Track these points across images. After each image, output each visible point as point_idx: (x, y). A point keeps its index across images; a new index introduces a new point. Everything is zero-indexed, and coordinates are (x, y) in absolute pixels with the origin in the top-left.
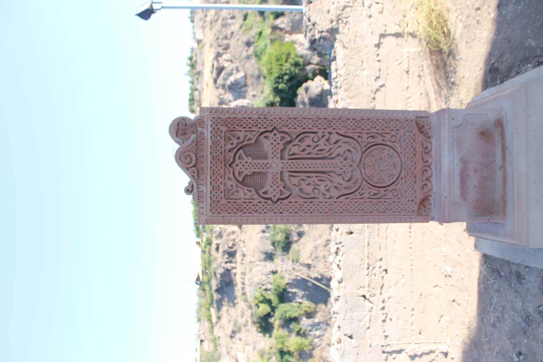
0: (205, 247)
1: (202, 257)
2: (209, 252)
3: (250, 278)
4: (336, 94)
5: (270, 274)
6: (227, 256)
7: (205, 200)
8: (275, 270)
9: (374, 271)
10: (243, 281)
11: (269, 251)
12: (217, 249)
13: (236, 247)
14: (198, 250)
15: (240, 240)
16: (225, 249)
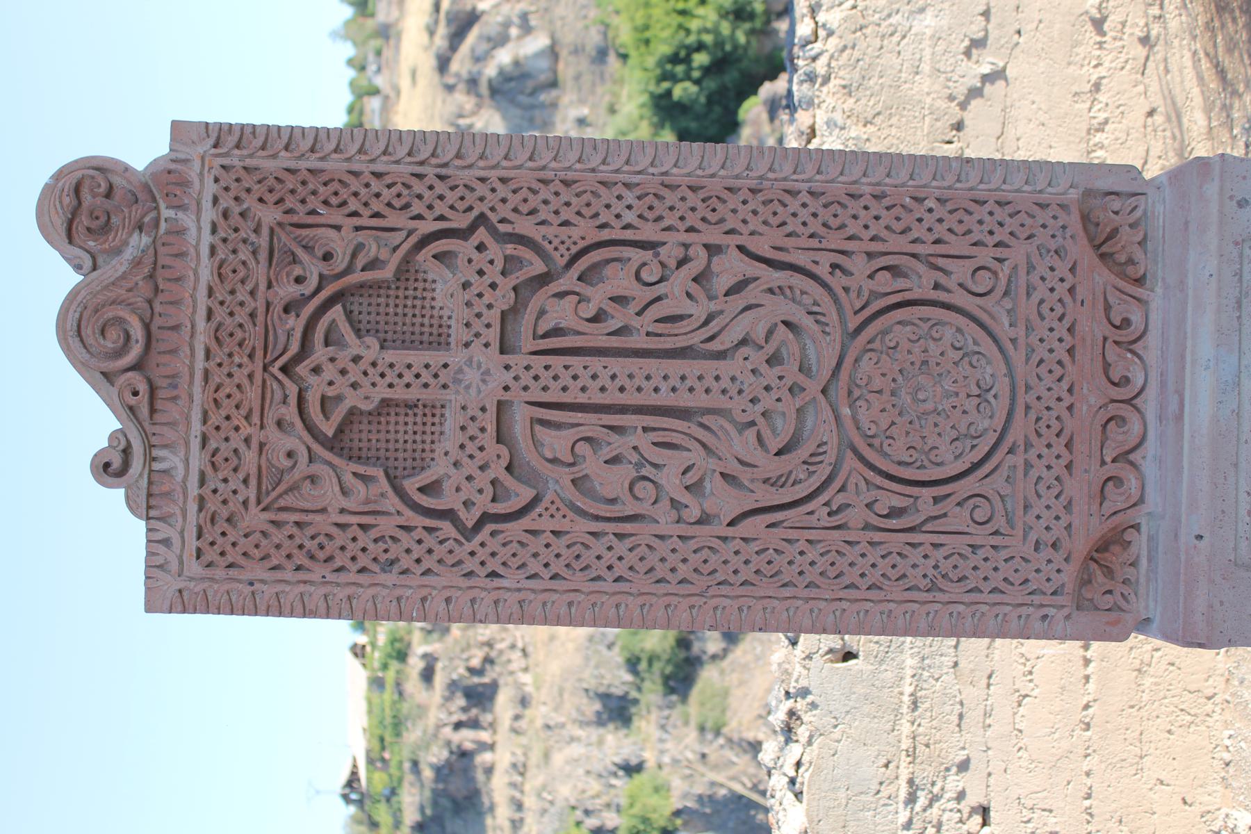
0: (385, 666)
1: (370, 702)
2: (398, 684)
3: (544, 787)
4: (810, 104)
5: (615, 775)
6: (461, 701)
7: (178, 512)
8: (634, 761)
9: (935, 811)
10: (518, 795)
11: (618, 691)
12: (428, 675)
13: (497, 669)
14: (357, 676)
15: (513, 647)
16: (455, 676)
